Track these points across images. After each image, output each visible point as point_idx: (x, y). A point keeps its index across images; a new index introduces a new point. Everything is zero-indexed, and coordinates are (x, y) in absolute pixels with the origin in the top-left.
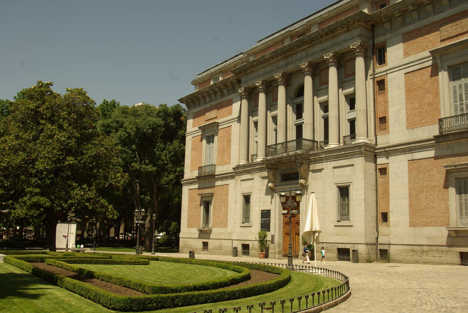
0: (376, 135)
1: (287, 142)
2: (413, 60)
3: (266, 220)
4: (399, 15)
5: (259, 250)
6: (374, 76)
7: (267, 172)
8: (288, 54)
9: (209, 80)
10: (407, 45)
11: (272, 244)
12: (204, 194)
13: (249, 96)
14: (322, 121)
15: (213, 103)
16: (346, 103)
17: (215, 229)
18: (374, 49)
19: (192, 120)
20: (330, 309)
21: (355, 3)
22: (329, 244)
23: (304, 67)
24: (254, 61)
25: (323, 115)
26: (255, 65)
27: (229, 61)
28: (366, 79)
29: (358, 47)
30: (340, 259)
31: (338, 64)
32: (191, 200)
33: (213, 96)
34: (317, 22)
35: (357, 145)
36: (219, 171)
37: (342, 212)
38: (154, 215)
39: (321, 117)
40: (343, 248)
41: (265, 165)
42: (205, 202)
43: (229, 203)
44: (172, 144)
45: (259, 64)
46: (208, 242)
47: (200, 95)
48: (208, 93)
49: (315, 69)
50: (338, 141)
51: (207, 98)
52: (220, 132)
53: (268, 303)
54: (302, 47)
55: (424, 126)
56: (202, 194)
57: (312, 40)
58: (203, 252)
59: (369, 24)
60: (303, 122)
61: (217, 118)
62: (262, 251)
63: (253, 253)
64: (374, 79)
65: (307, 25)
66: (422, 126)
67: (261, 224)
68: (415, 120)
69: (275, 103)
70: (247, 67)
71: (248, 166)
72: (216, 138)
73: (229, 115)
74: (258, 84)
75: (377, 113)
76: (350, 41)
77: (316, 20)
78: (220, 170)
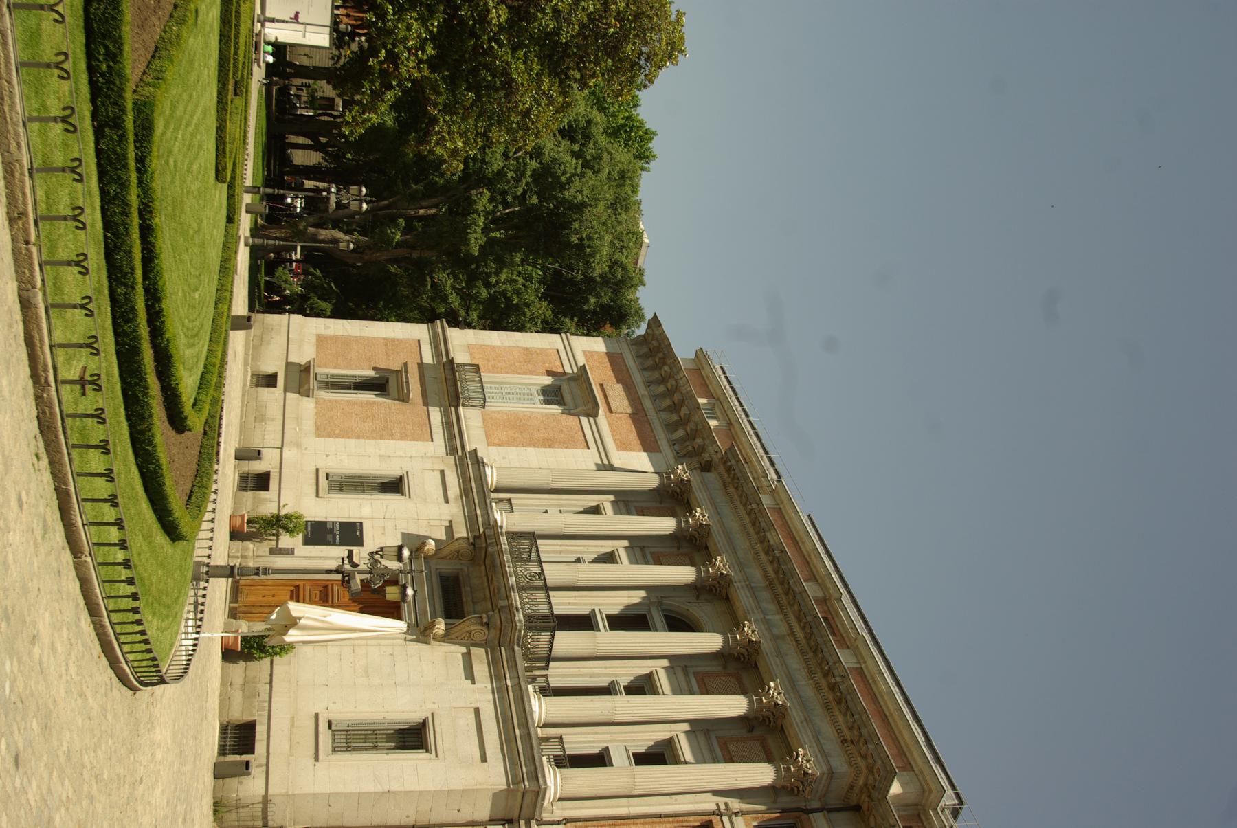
5: (253, 515)
6: (725, 815)
7: (465, 535)
8: (780, 589)
9: (709, 394)
11: (268, 549)
12: (407, 377)
13: (668, 492)
14: (603, 682)
15: (648, 404)
16: (652, 743)
18: (796, 814)
19: (604, 350)
20: (78, 583)
21: (915, 761)
22: (267, 699)
23: (746, 629)
24: (759, 503)
26: (750, 507)
27: (758, 444)
28: (717, 793)
29: (800, 768)
30: (225, 730)
31: (756, 718)
33: (668, 402)
34: (863, 666)
35: (539, 769)
36: (468, 417)
37: (356, 732)
39: (614, 679)
40: (255, 736)
41: (484, 532)
42: (384, 382)
43: (382, 442)
44: (540, 299)
45: (753, 515)
47: (669, 370)
48: (676, 389)
49: (742, 659)
50: (552, 720)
51: (662, 389)
52: (571, 421)
53: (101, 401)
54: (800, 625)
56: (406, 372)
57: (816, 650)
58: (250, 374)
59: (863, 798)
60: (599, 631)
61: (608, 413)
62: (249, 522)
63: (244, 500)
64: (718, 813)
65: (856, 639)
67: (325, 523)
69: (651, 560)
70: (744, 485)
71: (481, 489)
72: (556, 409)
73: (616, 444)
74: (701, 514)
76: (816, 748)
77: (869, 662)
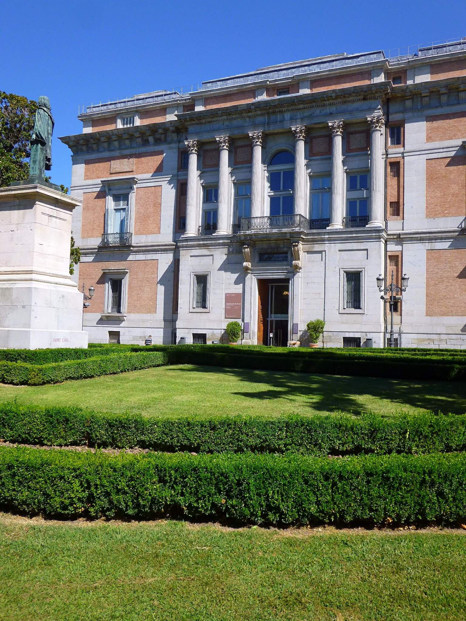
0: (386, 219)
2: (437, 146)
4: (428, 94)
47: (104, 138)
55: (447, 217)
66: (444, 216)
78: (140, 241)
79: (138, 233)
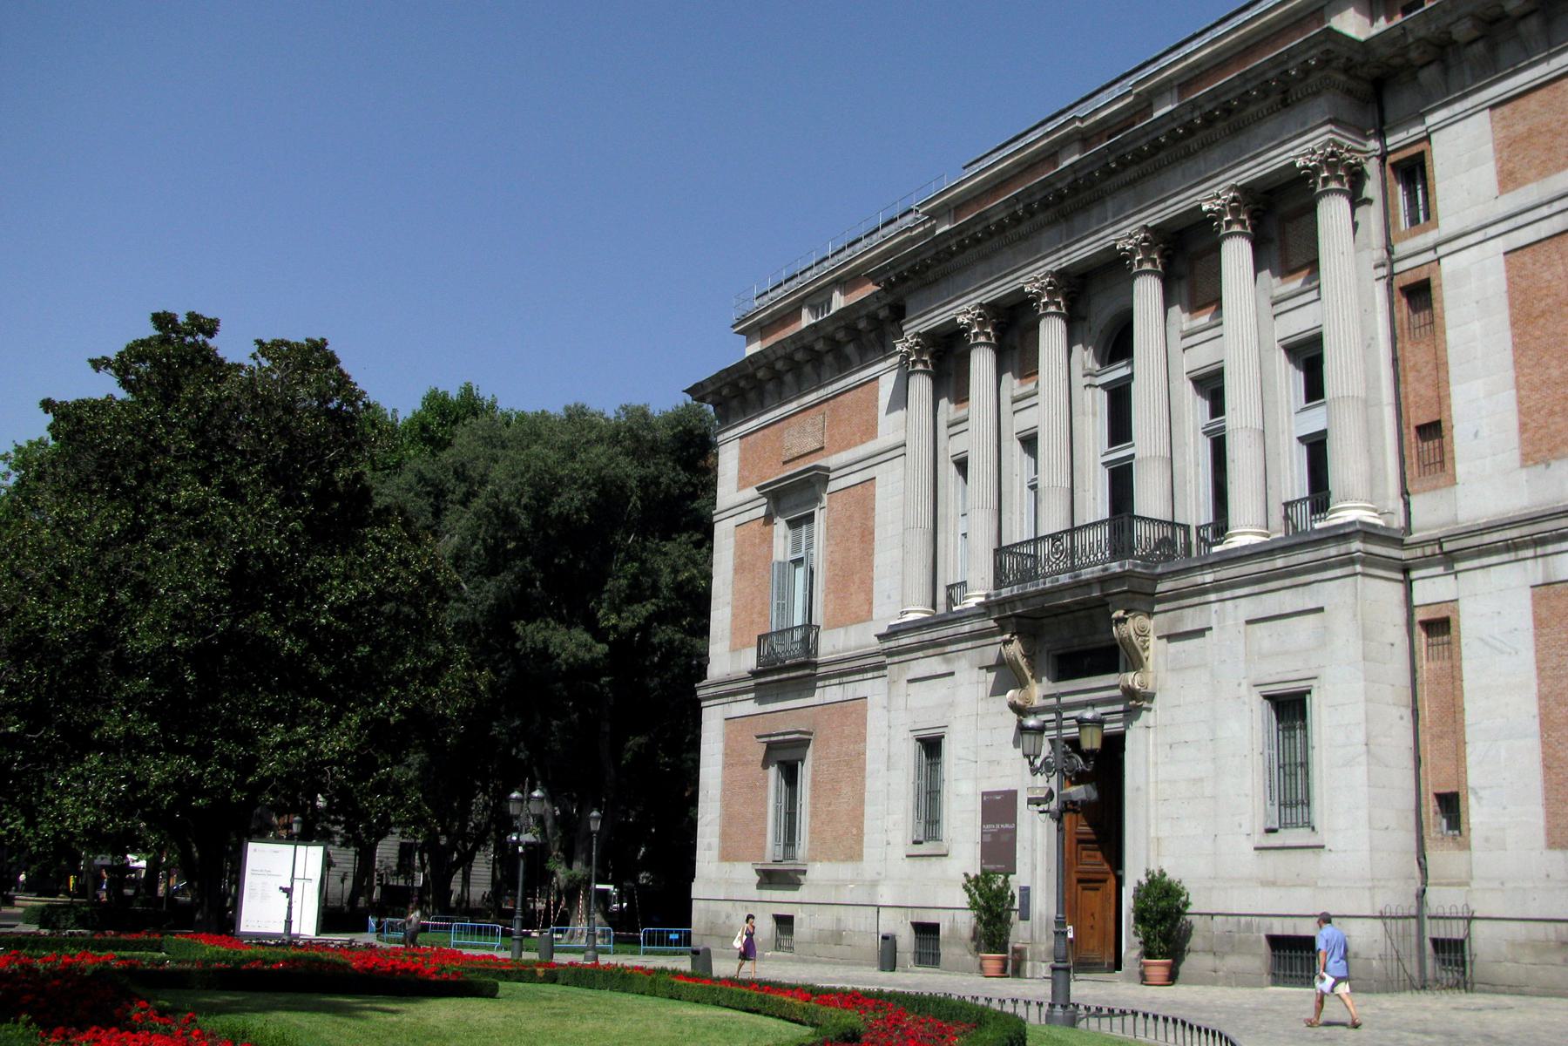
0: (1405, 493)
1: (1072, 531)
3: (1001, 830)
10: (1509, 146)
11: (1021, 922)
17: (818, 865)
25: (1208, 425)
32: (732, 758)
34: (1176, 83)
35: (1332, 533)
36: (831, 649)
38: (595, 814)
39: (1200, 431)
43: (869, 767)
46: (791, 918)
48: (789, 358)
68: (1553, 427)
73: (868, 440)
75: (1407, 407)
78: (834, 646)
79: (836, 623)
